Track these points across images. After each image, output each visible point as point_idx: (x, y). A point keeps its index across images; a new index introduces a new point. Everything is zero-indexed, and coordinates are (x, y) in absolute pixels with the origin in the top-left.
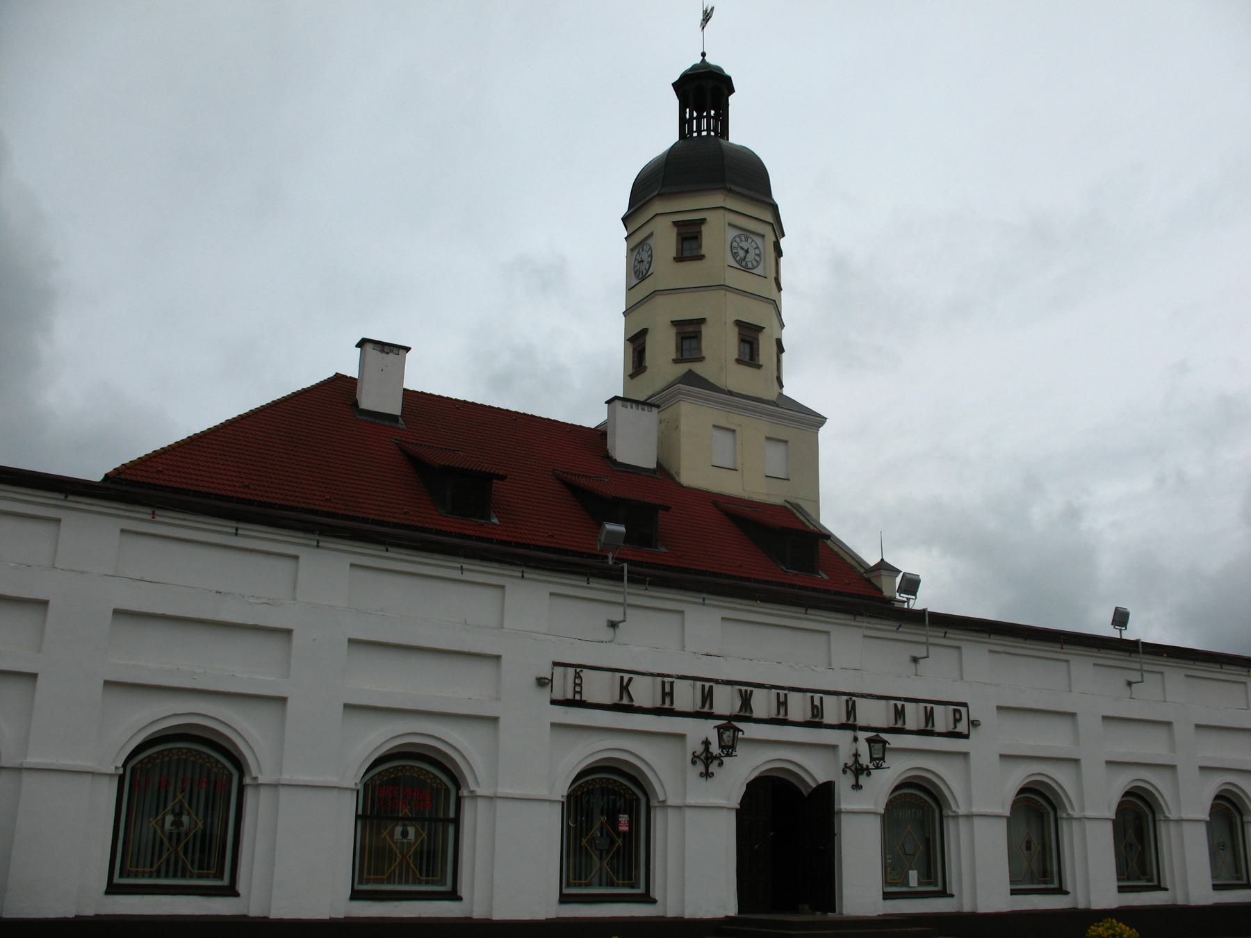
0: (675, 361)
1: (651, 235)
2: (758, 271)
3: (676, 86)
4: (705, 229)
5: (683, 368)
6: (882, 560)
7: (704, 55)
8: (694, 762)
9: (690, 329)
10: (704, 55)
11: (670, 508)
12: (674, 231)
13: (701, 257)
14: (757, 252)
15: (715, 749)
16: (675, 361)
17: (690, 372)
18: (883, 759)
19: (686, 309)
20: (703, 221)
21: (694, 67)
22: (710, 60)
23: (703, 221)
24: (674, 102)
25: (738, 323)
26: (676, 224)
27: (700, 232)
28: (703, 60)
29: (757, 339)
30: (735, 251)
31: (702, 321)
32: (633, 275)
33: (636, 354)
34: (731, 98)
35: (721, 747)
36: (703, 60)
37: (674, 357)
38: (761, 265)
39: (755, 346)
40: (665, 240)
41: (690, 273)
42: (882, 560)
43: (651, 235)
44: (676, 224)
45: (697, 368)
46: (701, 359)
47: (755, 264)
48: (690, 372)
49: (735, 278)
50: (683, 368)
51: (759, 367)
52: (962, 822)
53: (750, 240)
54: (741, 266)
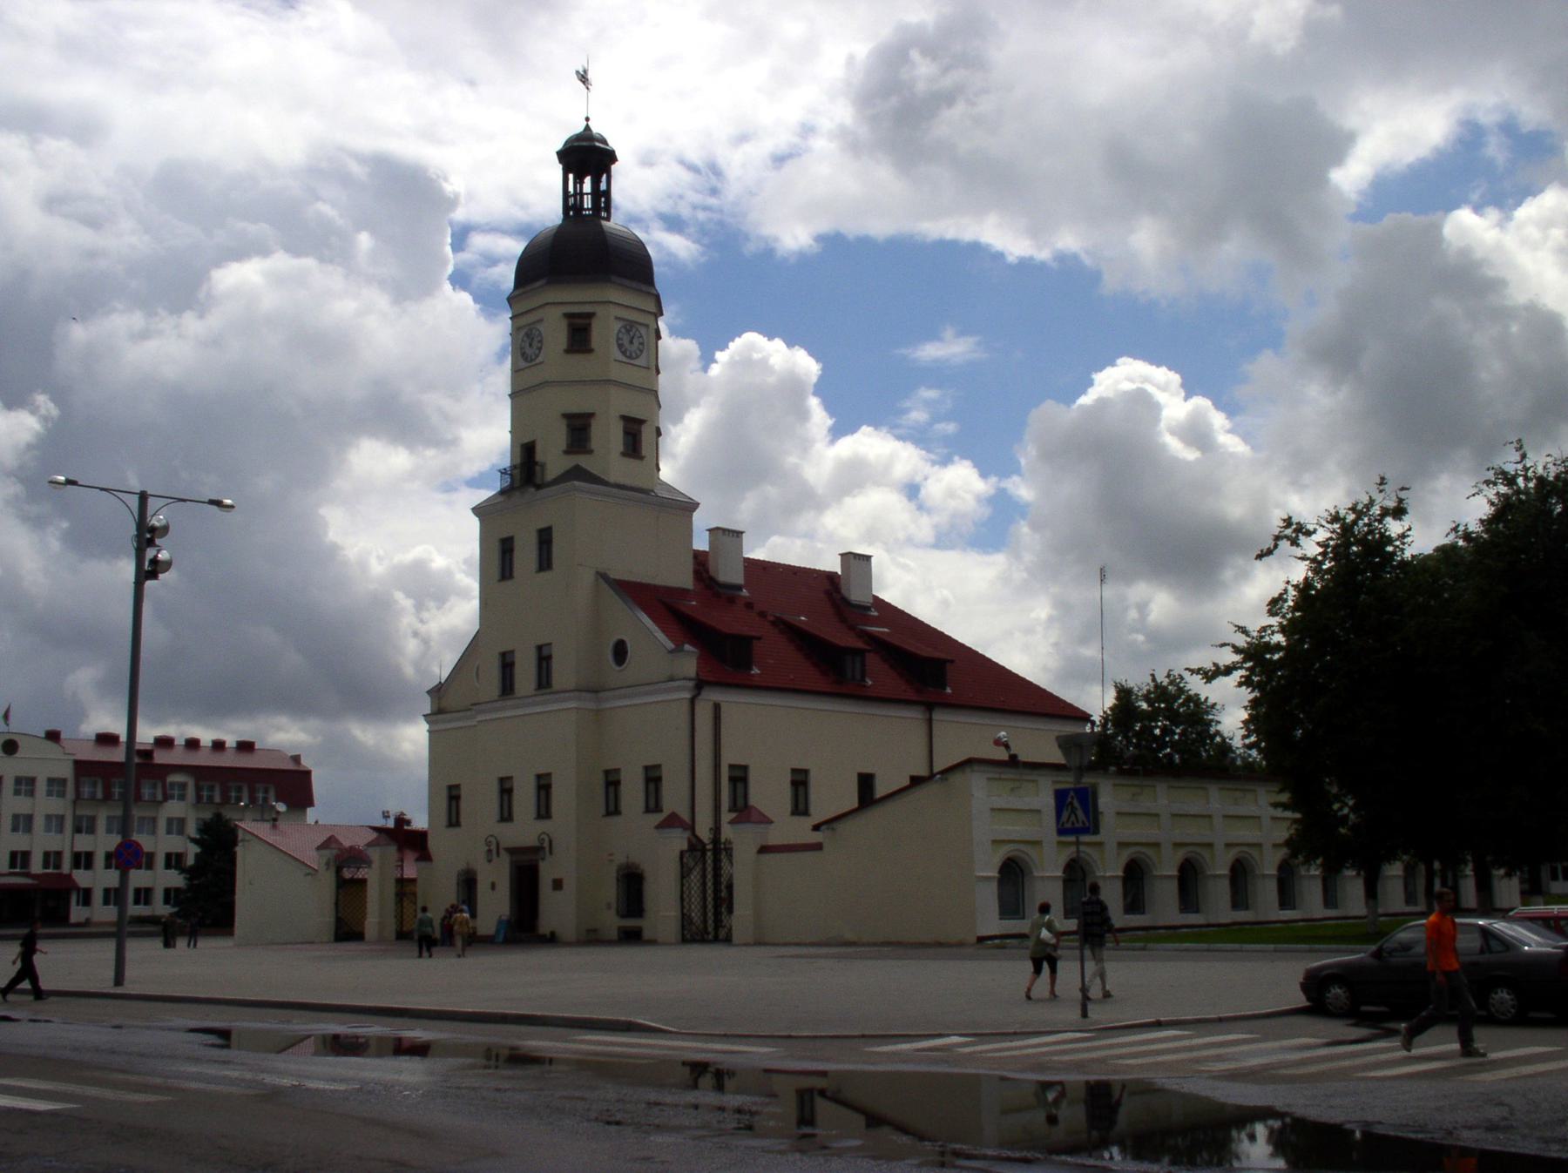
0: (567, 452)
1: (541, 320)
2: (641, 361)
7: (587, 119)
10: (587, 119)
16: (567, 452)
19: (576, 402)
20: (590, 316)
21: (578, 138)
22: (596, 129)
23: (590, 316)
24: (558, 170)
26: (568, 316)
27: (590, 324)
28: (587, 128)
29: (640, 432)
30: (620, 342)
31: (591, 415)
32: (520, 358)
34: (613, 167)
36: (587, 128)
38: (645, 354)
40: (555, 333)
41: (580, 366)
43: (541, 320)
44: (568, 316)
45: (583, 461)
46: (591, 452)
47: (638, 352)
49: (617, 372)
51: (641, 458)
54: (626, 356)
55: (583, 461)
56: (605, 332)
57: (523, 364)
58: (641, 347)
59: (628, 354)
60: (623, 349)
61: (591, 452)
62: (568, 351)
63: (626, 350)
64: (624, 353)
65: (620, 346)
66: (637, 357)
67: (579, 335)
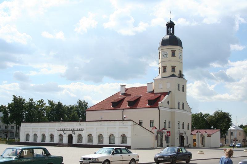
3: (167, 25)
4: (176, 52)
5: (173, 73)
12: (171, 52)
13: (175, 56)
16: (172, 72)
17: (173, 74)
19: (173, 64)
20: (175, 51)
23: (175, 51)
26: (172, 50)
36: (170, 20)
40: (170, 53)
44: (172, 50)
45: (174, 73)
48: (173, 74)
50: (173, 73)
55: (174, 73)
56: (177, 53)
57: (163, 57)
62: (172, 56)
67: (173, 54)
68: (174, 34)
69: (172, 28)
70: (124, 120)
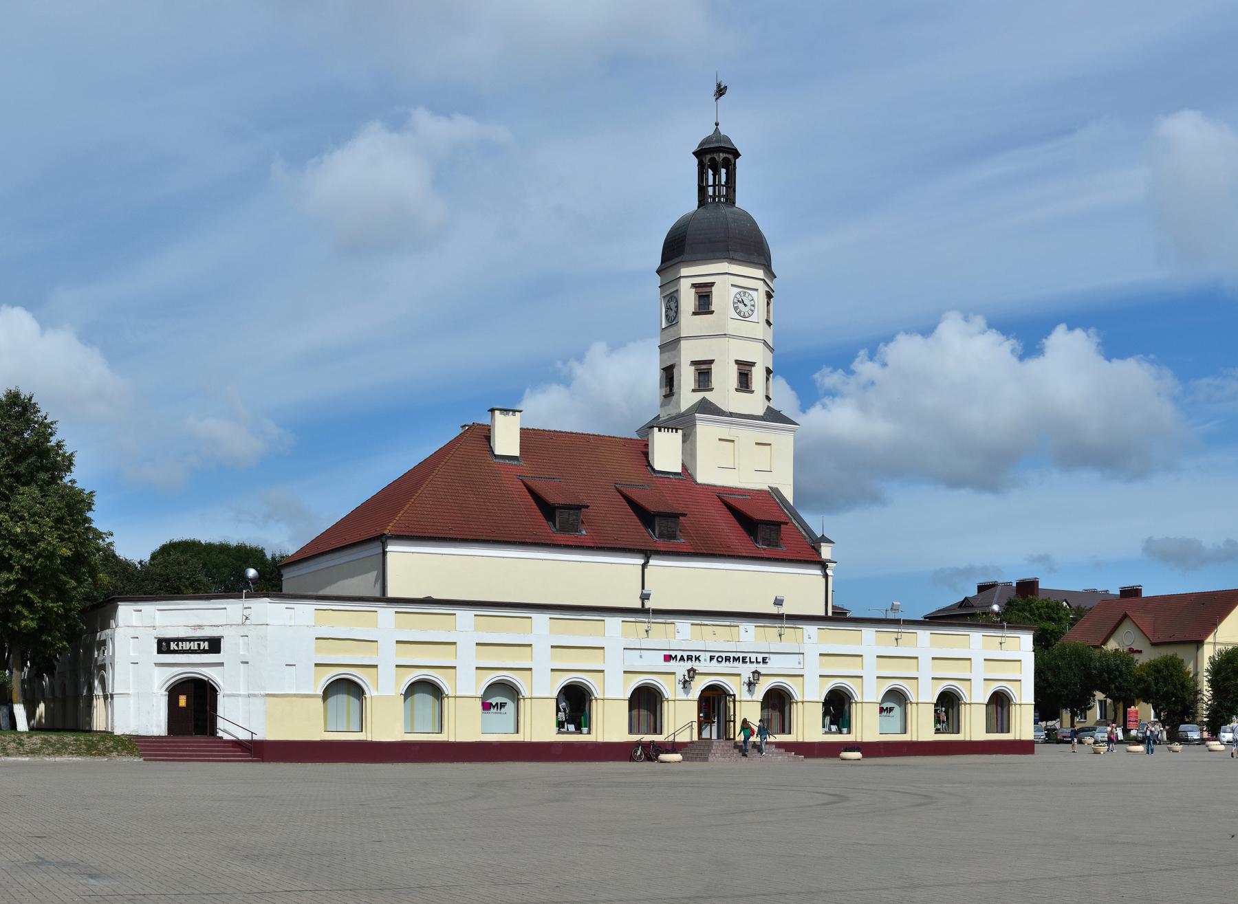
3: (696, 154)
5: (700, 395)
6: (823, 535)
7: (717, 124)
8: (679, 683)
9: (704, 367)
10: (717, 124)
11: (686, 514)
13: (712, 312)
14: (752, 308)
15: (687, 678)
18: (758, 680)
20: (712, 284)
22: (723, 131)
23: (712, 284)
25: (737, 362)
26: (694, 286)
30: (735, 305)
31: (711, 362)
33: (668, 380)
35: (689, 677)
37: (693, 388)
39: (749, 376)
40: (688, 299)
42: (823, 535)
47: (750, 312)
49: (734, 327)
52: (800, 704)
53: (747, 295)
55: (707, 395)
56: (722, 296)
58: (752, 308)
59: (742, 314)
60: (738, 311)
61: (712, 390)
63: (740, 312)
64: (739, 314)
65: (736, 308)
66: (750, 316)
68: (730, 200)
69: (723, 171)
70: (643, 611)
